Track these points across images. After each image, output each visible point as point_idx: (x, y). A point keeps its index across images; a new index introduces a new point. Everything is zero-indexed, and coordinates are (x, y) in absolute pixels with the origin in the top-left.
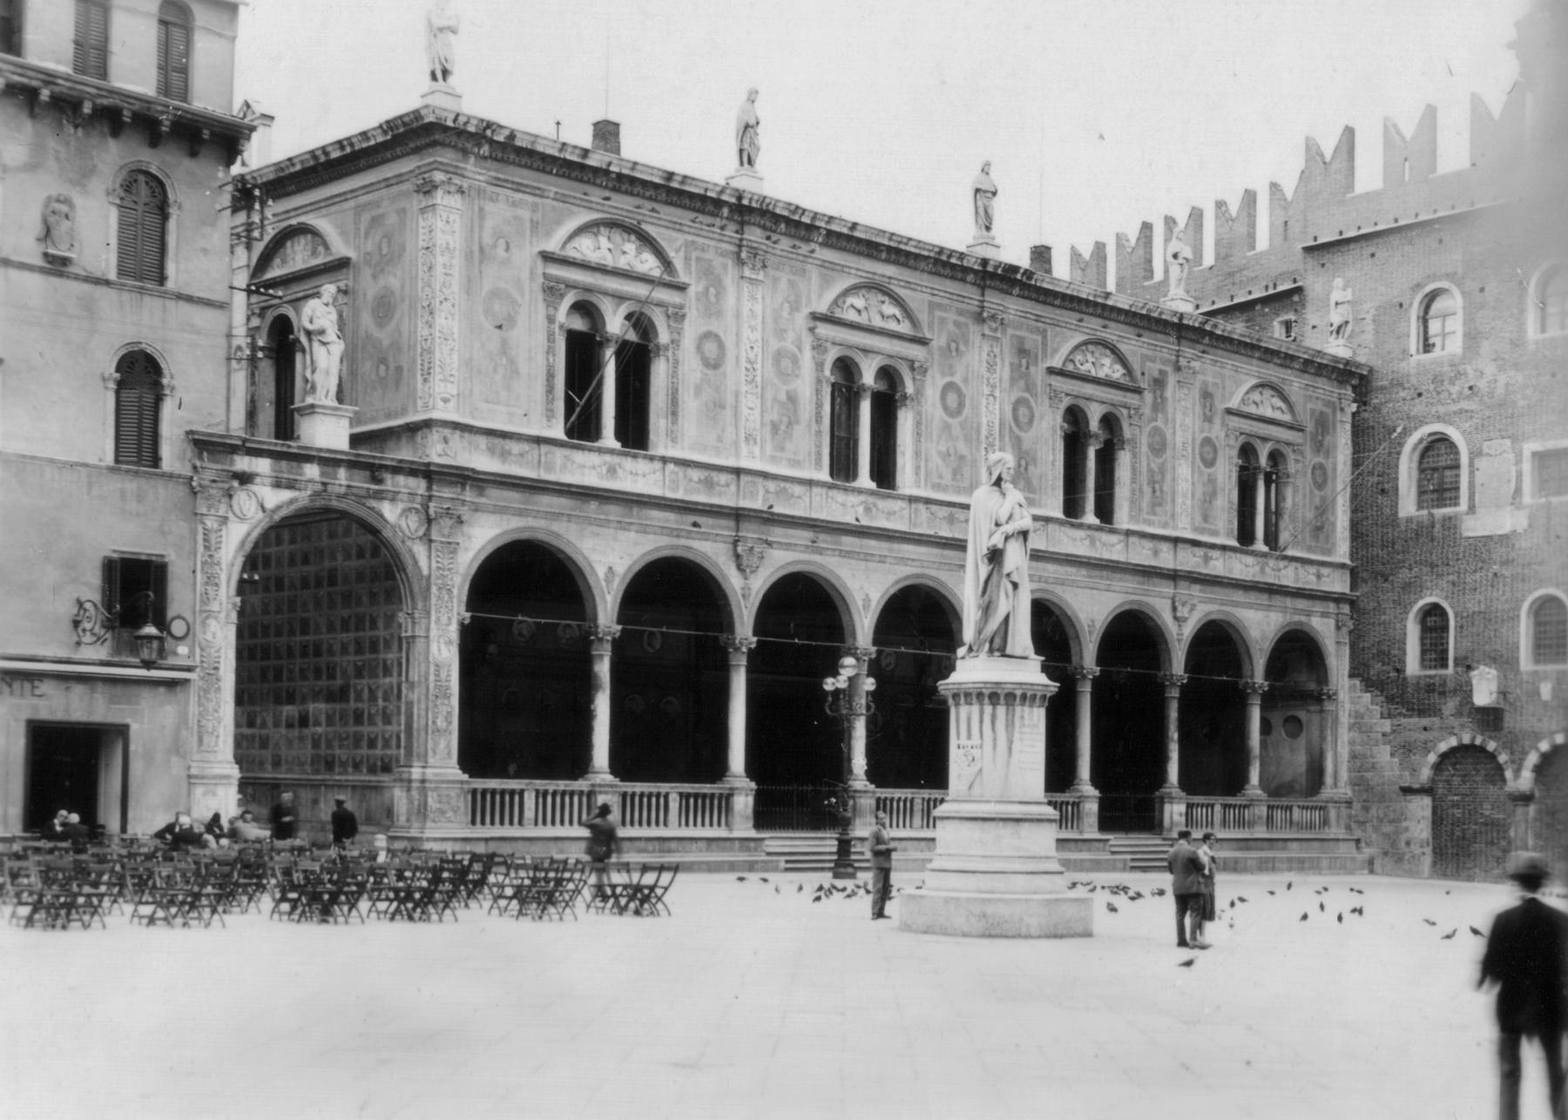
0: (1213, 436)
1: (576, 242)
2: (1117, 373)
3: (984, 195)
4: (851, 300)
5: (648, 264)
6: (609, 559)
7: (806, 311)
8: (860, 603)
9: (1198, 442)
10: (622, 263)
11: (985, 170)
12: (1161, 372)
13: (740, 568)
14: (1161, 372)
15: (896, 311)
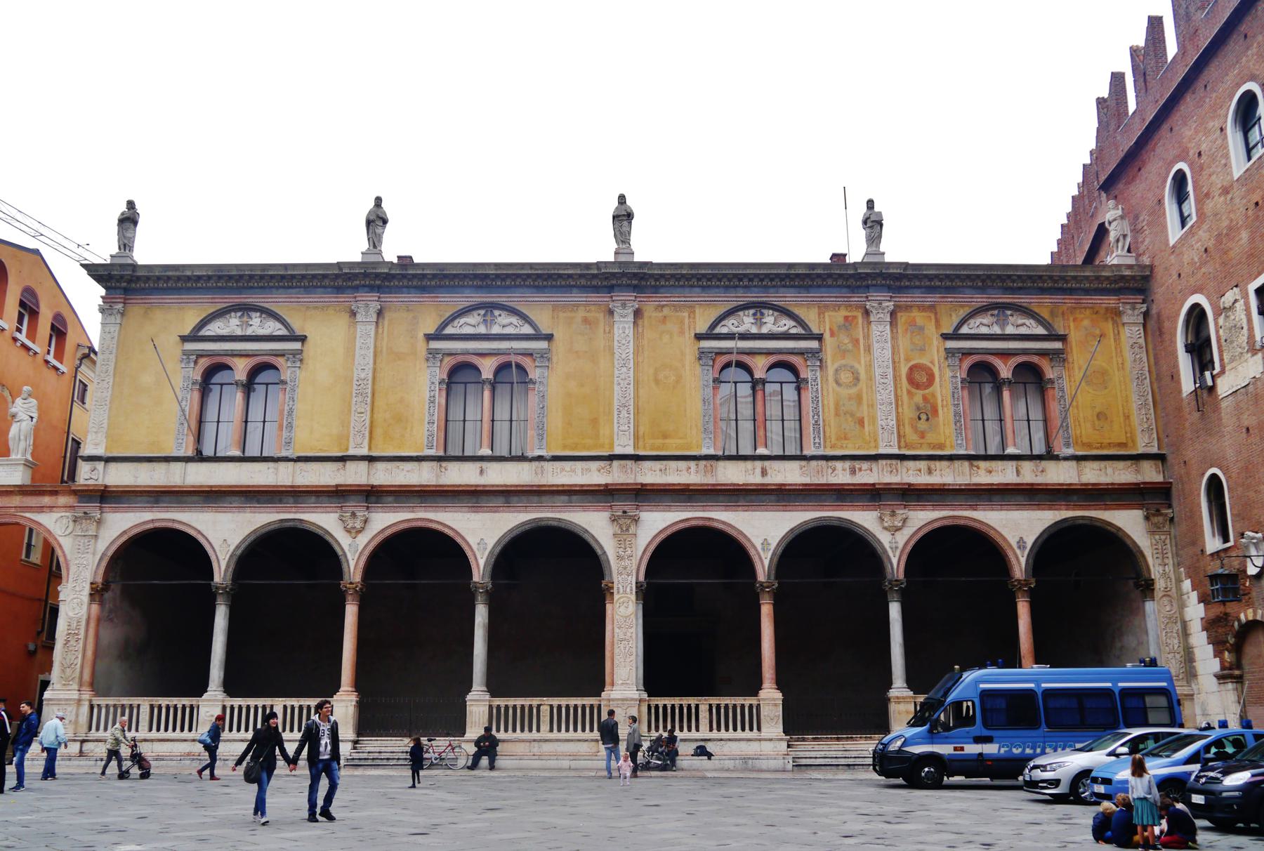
0: (924, 361)
1: (208, 327)
2: (786, 325)
3: (623, 217)
4: (462, 320)
5: (272, 327)
6: (224, 534)
7: (421, 335)
8: (475, 547)
9: (904, 370)
10: (249, 332)
11: (622, 199)
12: (846, 318)
13: (348, 531)
14: (846, 318)
15: (514, 320)
